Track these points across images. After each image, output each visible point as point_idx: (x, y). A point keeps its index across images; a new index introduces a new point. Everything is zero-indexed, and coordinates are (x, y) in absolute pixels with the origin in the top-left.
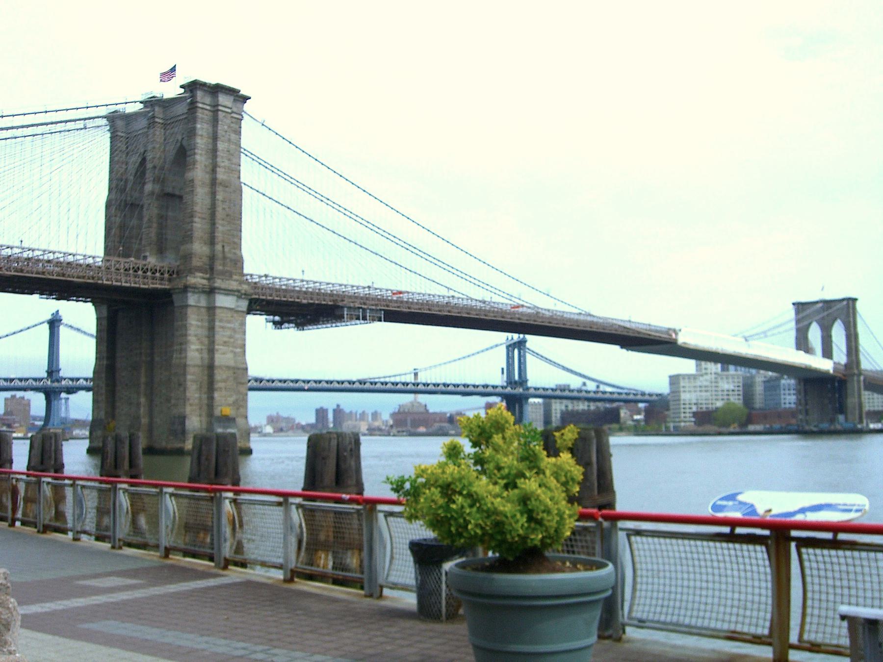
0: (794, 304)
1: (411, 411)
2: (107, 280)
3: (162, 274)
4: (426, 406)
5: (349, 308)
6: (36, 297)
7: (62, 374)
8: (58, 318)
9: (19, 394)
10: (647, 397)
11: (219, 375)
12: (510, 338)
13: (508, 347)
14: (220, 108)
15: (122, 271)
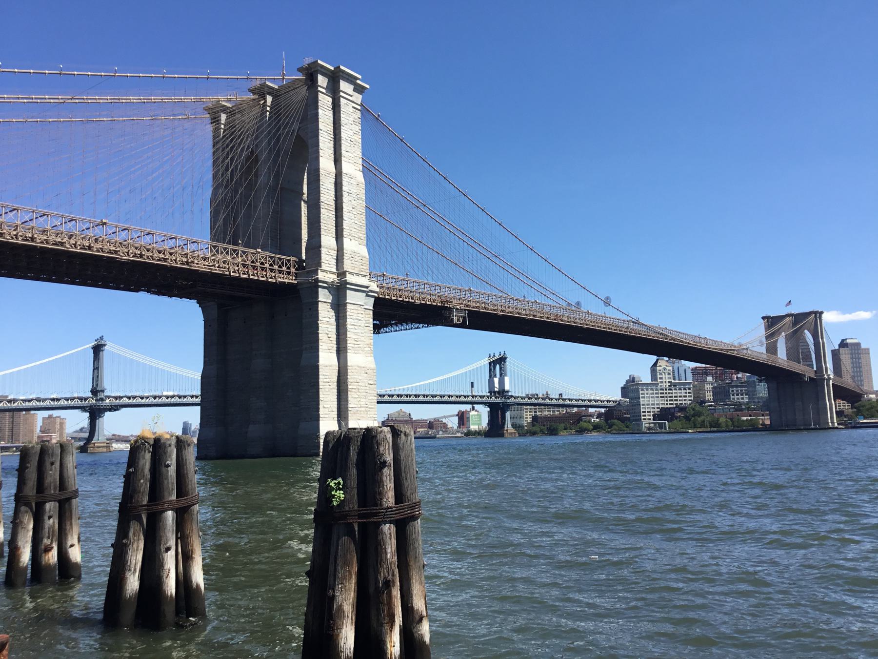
0: (763, 318)
1: (398, 419)
2: (234, 272)
3: (288, 268)
4: (410, 414)
5: (457, 309)
6: (143, 295)
7: (106, 393)
8: (103, 342)
9: (55, 413)
10: (606, 404)
11: (352, 376)
12: (492, 355)
13: (490, 363)
14: (342, 94)
15: (249, 262)
